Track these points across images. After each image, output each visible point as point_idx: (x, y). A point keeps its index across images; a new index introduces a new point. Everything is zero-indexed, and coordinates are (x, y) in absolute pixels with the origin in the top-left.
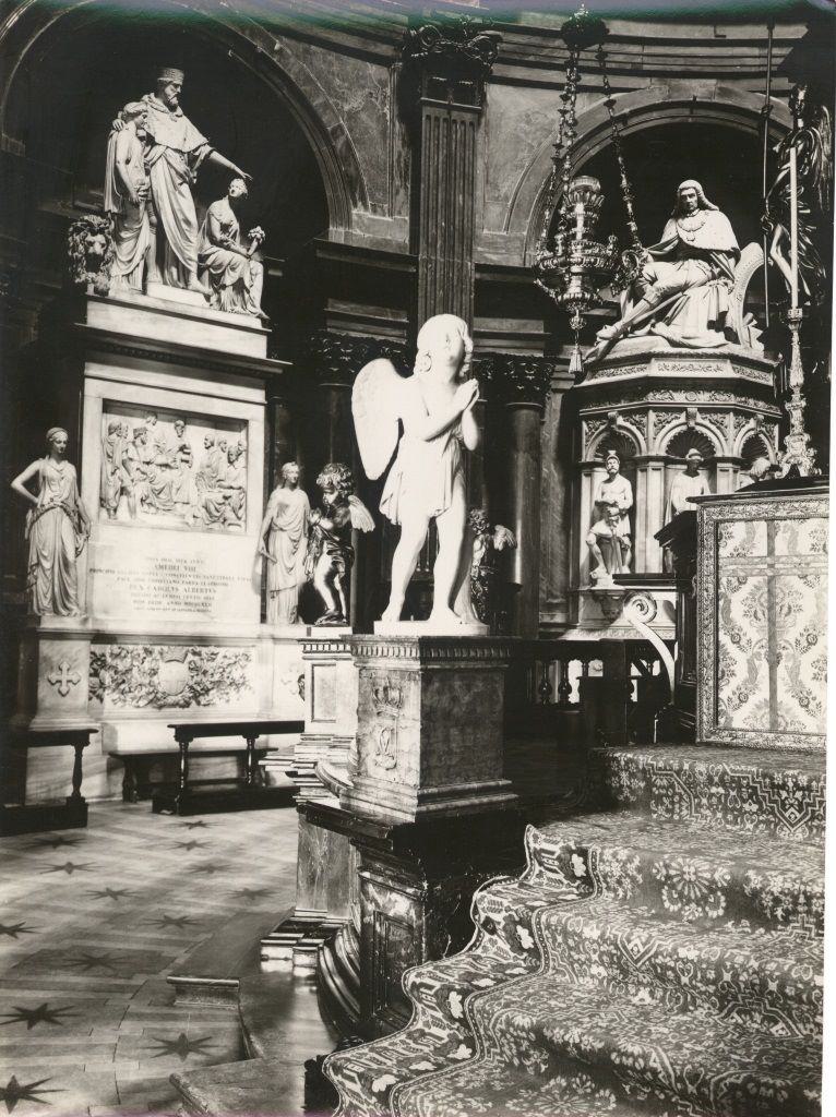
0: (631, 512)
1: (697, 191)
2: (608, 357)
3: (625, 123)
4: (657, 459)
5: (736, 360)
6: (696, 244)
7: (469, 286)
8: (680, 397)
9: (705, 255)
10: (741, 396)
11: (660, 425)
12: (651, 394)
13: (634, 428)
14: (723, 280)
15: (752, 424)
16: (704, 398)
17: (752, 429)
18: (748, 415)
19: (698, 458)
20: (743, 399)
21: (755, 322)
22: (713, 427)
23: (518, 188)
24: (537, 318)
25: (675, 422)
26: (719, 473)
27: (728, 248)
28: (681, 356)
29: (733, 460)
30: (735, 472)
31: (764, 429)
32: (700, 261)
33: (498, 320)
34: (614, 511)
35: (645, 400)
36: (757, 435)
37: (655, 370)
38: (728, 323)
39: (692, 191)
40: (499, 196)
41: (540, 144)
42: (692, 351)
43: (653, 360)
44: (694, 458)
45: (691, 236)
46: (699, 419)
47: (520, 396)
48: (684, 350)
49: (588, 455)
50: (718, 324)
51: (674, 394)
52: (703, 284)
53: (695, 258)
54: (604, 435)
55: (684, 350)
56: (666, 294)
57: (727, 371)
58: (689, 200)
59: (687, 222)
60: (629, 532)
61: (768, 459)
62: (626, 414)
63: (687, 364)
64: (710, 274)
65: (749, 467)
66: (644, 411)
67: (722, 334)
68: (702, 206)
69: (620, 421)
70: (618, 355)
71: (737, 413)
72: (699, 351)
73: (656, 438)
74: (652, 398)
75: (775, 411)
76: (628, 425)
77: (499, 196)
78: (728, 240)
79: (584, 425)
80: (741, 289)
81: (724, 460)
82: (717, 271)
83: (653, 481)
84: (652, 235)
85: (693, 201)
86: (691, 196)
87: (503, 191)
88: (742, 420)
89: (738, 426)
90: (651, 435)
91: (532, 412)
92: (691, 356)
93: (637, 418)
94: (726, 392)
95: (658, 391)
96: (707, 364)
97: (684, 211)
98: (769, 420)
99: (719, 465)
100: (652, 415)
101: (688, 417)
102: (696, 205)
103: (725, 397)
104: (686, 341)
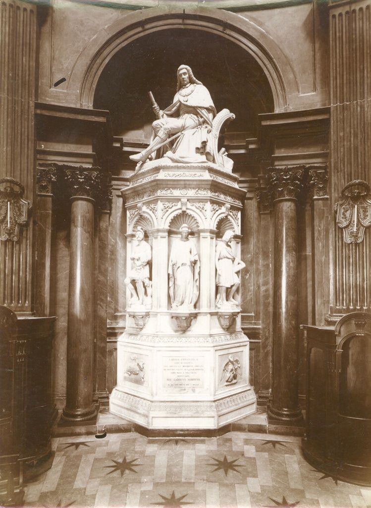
0: (150, 263)
1: (188, 71)
2: (142, 171)
3: (143, 27)
4: (163, 231)
5: (211, 170)
6: (189, 104)
7: (32, 117)
8: (176, 193)
9: (194, 110)
10: (215, 192)
11: (166, 209)
12: (159, 191)
13: (151, 213)
14: (205, 125)
15: (223, 209)
16: (191, 193)
17: (224, 213)
18: (220, 204)
19: (187, 229)
20: (217, 194)
21: (226, 153)
22: (198, 211)
23: (75, 64)
24: (88, 144)
25: (174, 208)
26: (201, 238)
27: (207, 105)
28: (178, 168)
29: (211, 232)
30: (212, 238)
31: (231, 214)
32: (191, 115)
33: (61, 144)
34: (138, 263)
35: (156, 195)
36: (226, 217)
37: (162, 175)
38: (208, 149)
39: (185, 71)
40: (62, 68)
41: (90, 39)
42: (184, 165)
43: (161, 170)
44: (184, 229)
45: (185, 99)
46: (189, 205)
47: (77, 191)
48: (180, 165)
49: (129, 231)
50: (202, 149)
51: (173, 191)
52: (193, 128)
53: (188, 113)
54: (137, 218)
55: (180, 165)
56: (170, 135)
57: (207, 176)
58: (183, 76)
59: (184, 91)
60: (149, 276)
61: (234, 231)
62: (148, 203)
63: (182, 173)
64: (197, 122)
65: (221, 237)
66: (155, 201)
67: (204, 157)
68: (192, 82)
69: (144, 209)
70: (146, 170)
71: (213, 202)
72: (189, 165)
73: (160, 218)
74: (159, 193)
75: (238, 204)
76: (148, 211)
77: (62, 68)
78: (207, 101)
79: (128, 212)
80: (216, 132)
81: (204, 231)
82: (201, 120)
83: (160, 243)
84: (165, 102)
85: (186, 77)
86: (185, 74)
87: (65, 66)
88: (216, 207)
89: (215, 211)
90: (159, 218)
91: (84, 203)
92: (184, 168)
93: (152, 206)
94: (205, 189)
95: (163, 188)
96: (193, 173)
97: (182, 86)
98: (233, 208)
99: (201, 234)
100: (160, 205)
101: (182, 204)
102: (188, 80)
103: (205, 192)
104: (181, 159)
